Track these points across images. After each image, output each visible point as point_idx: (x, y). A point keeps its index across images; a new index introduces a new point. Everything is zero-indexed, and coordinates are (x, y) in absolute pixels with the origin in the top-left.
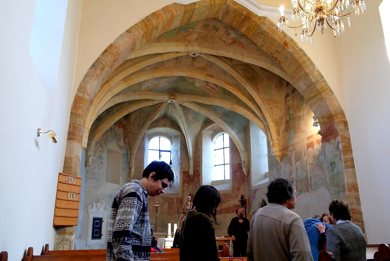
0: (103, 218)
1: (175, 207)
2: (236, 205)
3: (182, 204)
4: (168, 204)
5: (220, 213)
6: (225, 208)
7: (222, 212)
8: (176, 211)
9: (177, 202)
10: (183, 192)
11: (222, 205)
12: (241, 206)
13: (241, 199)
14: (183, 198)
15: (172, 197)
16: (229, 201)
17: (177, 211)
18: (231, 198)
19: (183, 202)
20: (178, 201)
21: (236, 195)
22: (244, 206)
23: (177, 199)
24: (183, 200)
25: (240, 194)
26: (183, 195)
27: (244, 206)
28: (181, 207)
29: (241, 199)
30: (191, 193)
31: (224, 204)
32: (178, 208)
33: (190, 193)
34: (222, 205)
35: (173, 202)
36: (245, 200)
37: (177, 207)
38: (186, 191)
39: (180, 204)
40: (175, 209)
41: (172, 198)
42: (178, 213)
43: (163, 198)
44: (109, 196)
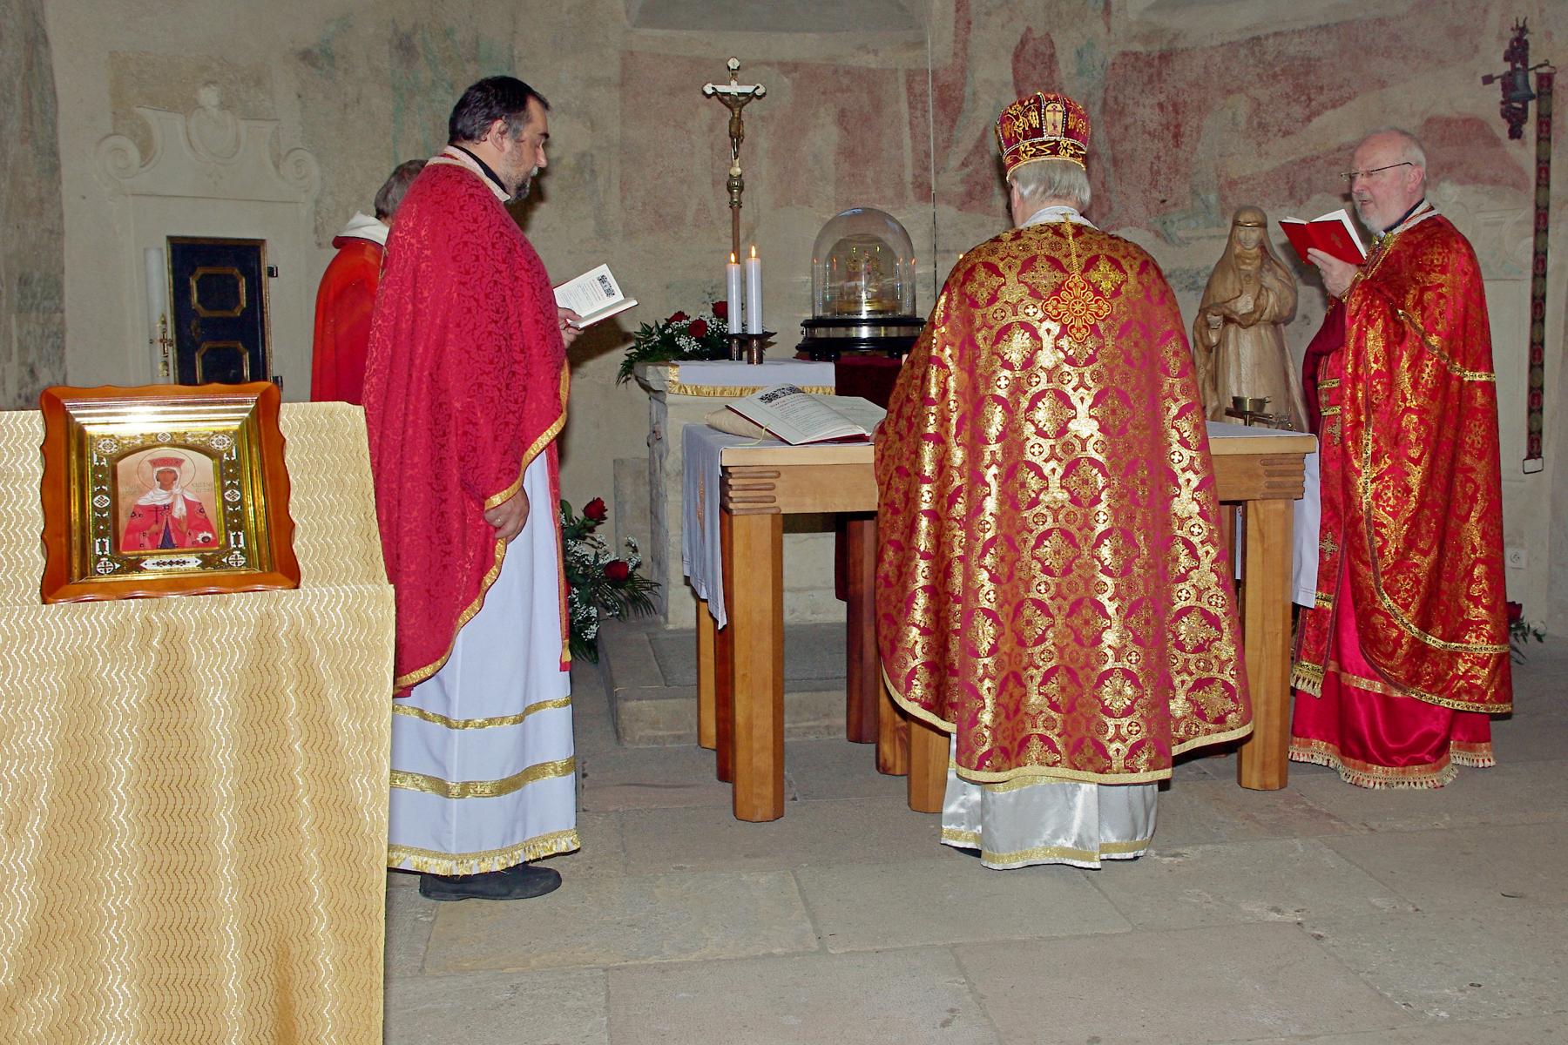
0: (268, 242)
1: (899, 147)
2: (1448, 122)
3: (954, 121)
4: (842, 117)
5: (1291, 195)
6: (1339, 149)
7: (1309, 180)
8: (908, 177)
9: (912, 106)
10: (970, 23)
11: (1308, 119)
12: (1501, 128)
13: (1507, 67)
14: (963, 70)
15: (873, 66)
16: (1382, 84)
17: (913, 183)
18: (1404, 58)
19: (967, 106)
20: (924, 93)
21: (1456, 33)
22: (1530, 129)
23: (911, 76)
24: (968, 91)
25: (1494, 18)
26: (965, 42)
27: (1530, 129)
28: (948, 144)
29: (1507, 67)
30: (1029, 29)
31: (1329, 113)
32: (927, 155)
33: (1022, 30)
34: (1316, 122)
35: (878, 106)
36: (1541, 77)
37: (914, 149)
38: (988, 14)
39: (935, 122)
40: (902, 166)
41: (869, 70)
42: (925, 193)
43: (796, 75)
44: (306, 56)
